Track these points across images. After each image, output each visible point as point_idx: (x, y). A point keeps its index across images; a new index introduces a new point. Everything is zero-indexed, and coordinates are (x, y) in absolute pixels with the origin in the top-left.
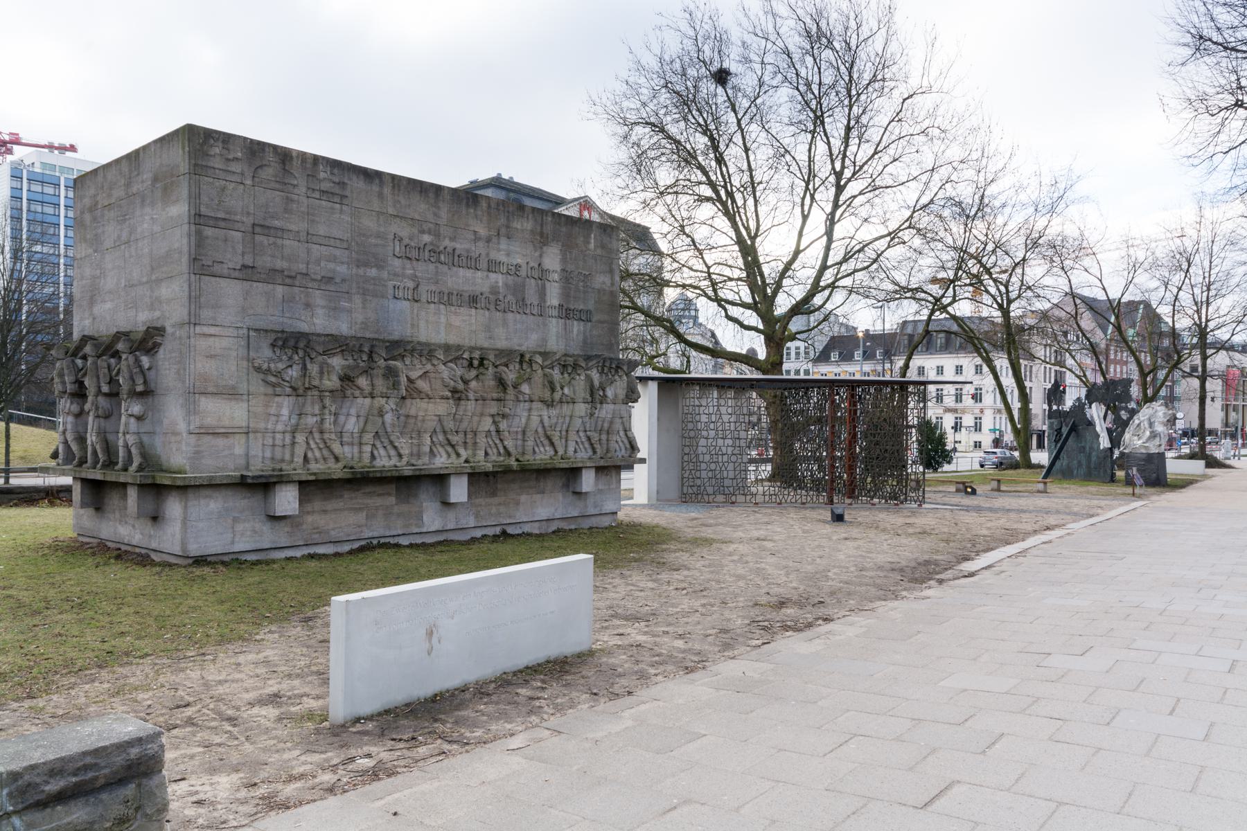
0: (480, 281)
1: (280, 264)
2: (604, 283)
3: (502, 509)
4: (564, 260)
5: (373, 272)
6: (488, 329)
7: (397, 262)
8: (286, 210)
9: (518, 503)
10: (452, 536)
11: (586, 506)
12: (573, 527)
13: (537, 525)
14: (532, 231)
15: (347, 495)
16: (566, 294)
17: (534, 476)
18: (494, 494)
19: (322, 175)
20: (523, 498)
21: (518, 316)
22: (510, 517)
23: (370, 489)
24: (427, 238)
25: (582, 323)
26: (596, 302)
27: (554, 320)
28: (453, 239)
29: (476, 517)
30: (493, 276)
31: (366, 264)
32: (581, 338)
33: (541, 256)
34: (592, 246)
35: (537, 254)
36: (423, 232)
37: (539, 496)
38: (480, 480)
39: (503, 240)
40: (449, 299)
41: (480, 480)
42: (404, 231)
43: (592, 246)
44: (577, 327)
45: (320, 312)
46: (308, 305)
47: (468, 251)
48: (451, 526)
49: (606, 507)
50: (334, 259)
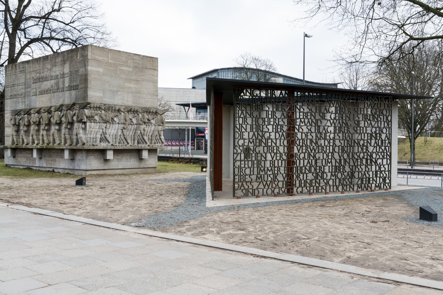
0: (47, 85)
1: (15, 93)
2: (83, 71)
3: (52, 162)
4: (70, 68)
5: (29, 90)
6: (50, 100)
7: (33, 85)
8: (16, 79)
9: (56, 161)
10: (40, 169)
11: (75, 166)
12: (72, 173)
13: (62, 170)
14: (61, 61)
15: (24, 153)
16: (71, 81)
17: (60, 151)
18: (50, 157)
19: (21, 67)
20: (57, 159)
21: (57, 93)
22: (54, 165)
23: (27, 152)
24: (38, 75)
25: (75, 91)
26: (80, 80)
27: (67, 92)
28: (43, 73)
29: (46, 164)
30: (51, 81)
31: (28, 88)
32: (75, 97)
33: (63, 69)
34: (79, 57)
35: (62, 69)
36: (37, 74)
37: (61, 159)
38: (41, 151)
39: (54, 67)
40: (42, 93)
41: (41, 151)
42: (33, 75)
43: (79, 57)
44: (73, 93)
45: (20, 103)
46: (19, 102)
47: (46, 75)
48: (41, 166)
49: (81, 167)
50: (22, 89)
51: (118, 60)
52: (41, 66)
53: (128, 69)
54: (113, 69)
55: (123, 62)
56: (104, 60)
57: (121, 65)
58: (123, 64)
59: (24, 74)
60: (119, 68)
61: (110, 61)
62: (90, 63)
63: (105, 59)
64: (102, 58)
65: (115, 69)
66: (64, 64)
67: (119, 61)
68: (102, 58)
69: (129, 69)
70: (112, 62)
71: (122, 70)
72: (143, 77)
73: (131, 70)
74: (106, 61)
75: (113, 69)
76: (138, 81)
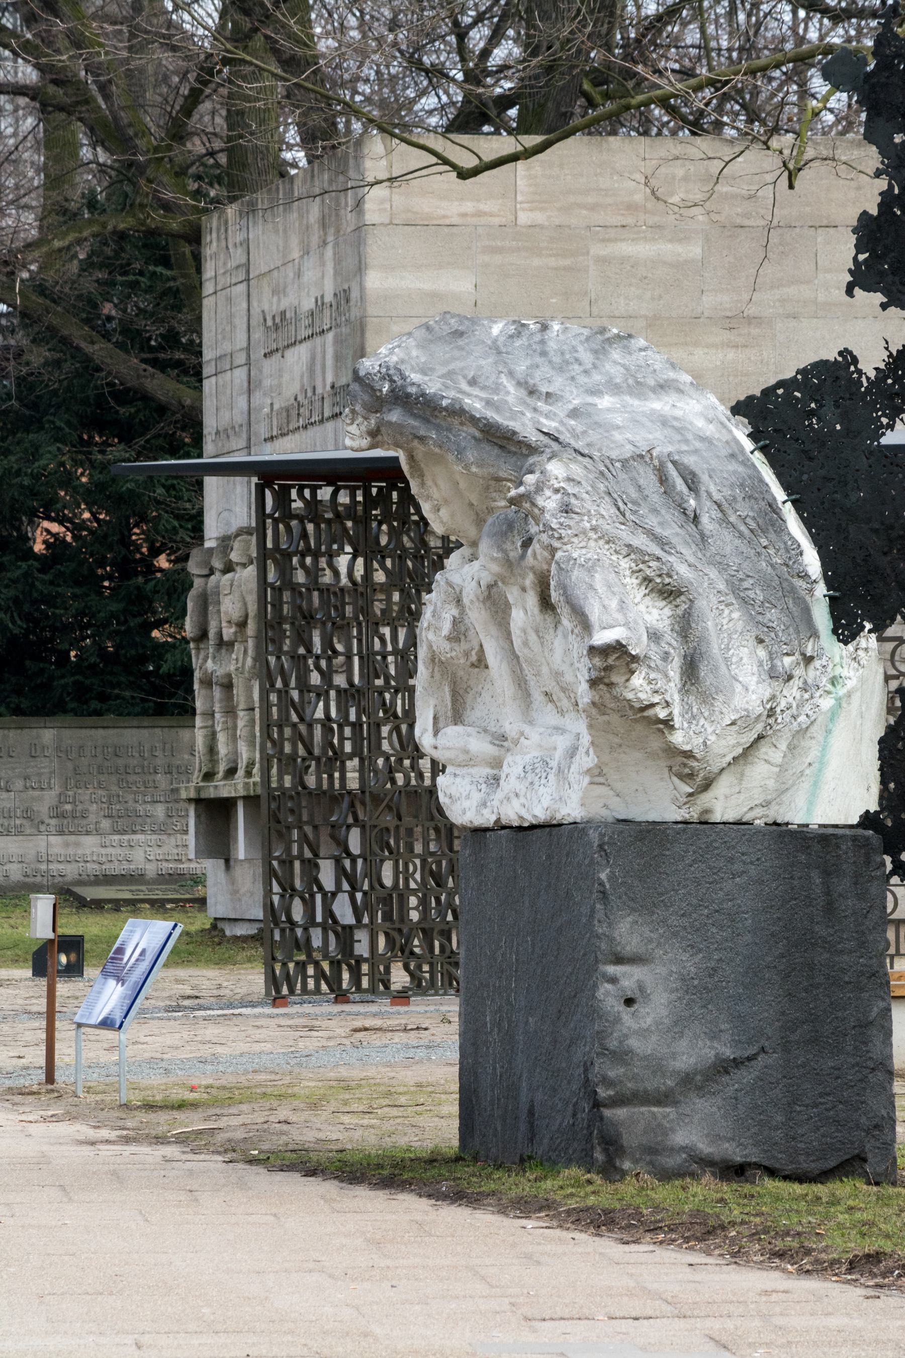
7: (269, 366)
51: (590, 199)
52: (281, 243)
53: (667, 249)
54: (552, 262)
55: (631, 207)
56: (480, 214)
57: (612, 233)
58: (630, 220)
59: (242, 287)
60: (597, 250)
61: (524, 218)
62: (374, 250)
63: (485, 207)
64: (469, 207)
65: (567, 262)
66: (325, 243)
67: (593, 208)
68: (469, 207)
69: (679, 248)
70: (539, 217)
71: (623, 260)
72: (791, 291)
73: (694, 250)
74: (496, 221)
75: (552, 262)
76: (751, 320)
